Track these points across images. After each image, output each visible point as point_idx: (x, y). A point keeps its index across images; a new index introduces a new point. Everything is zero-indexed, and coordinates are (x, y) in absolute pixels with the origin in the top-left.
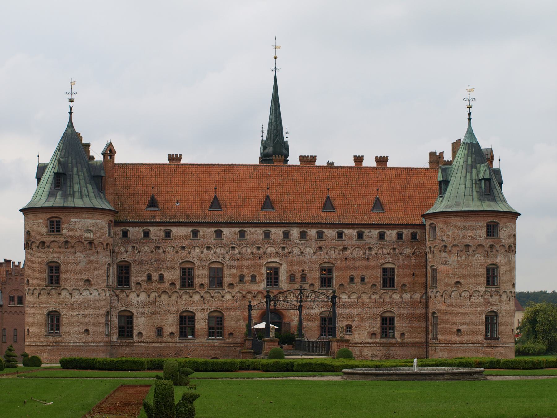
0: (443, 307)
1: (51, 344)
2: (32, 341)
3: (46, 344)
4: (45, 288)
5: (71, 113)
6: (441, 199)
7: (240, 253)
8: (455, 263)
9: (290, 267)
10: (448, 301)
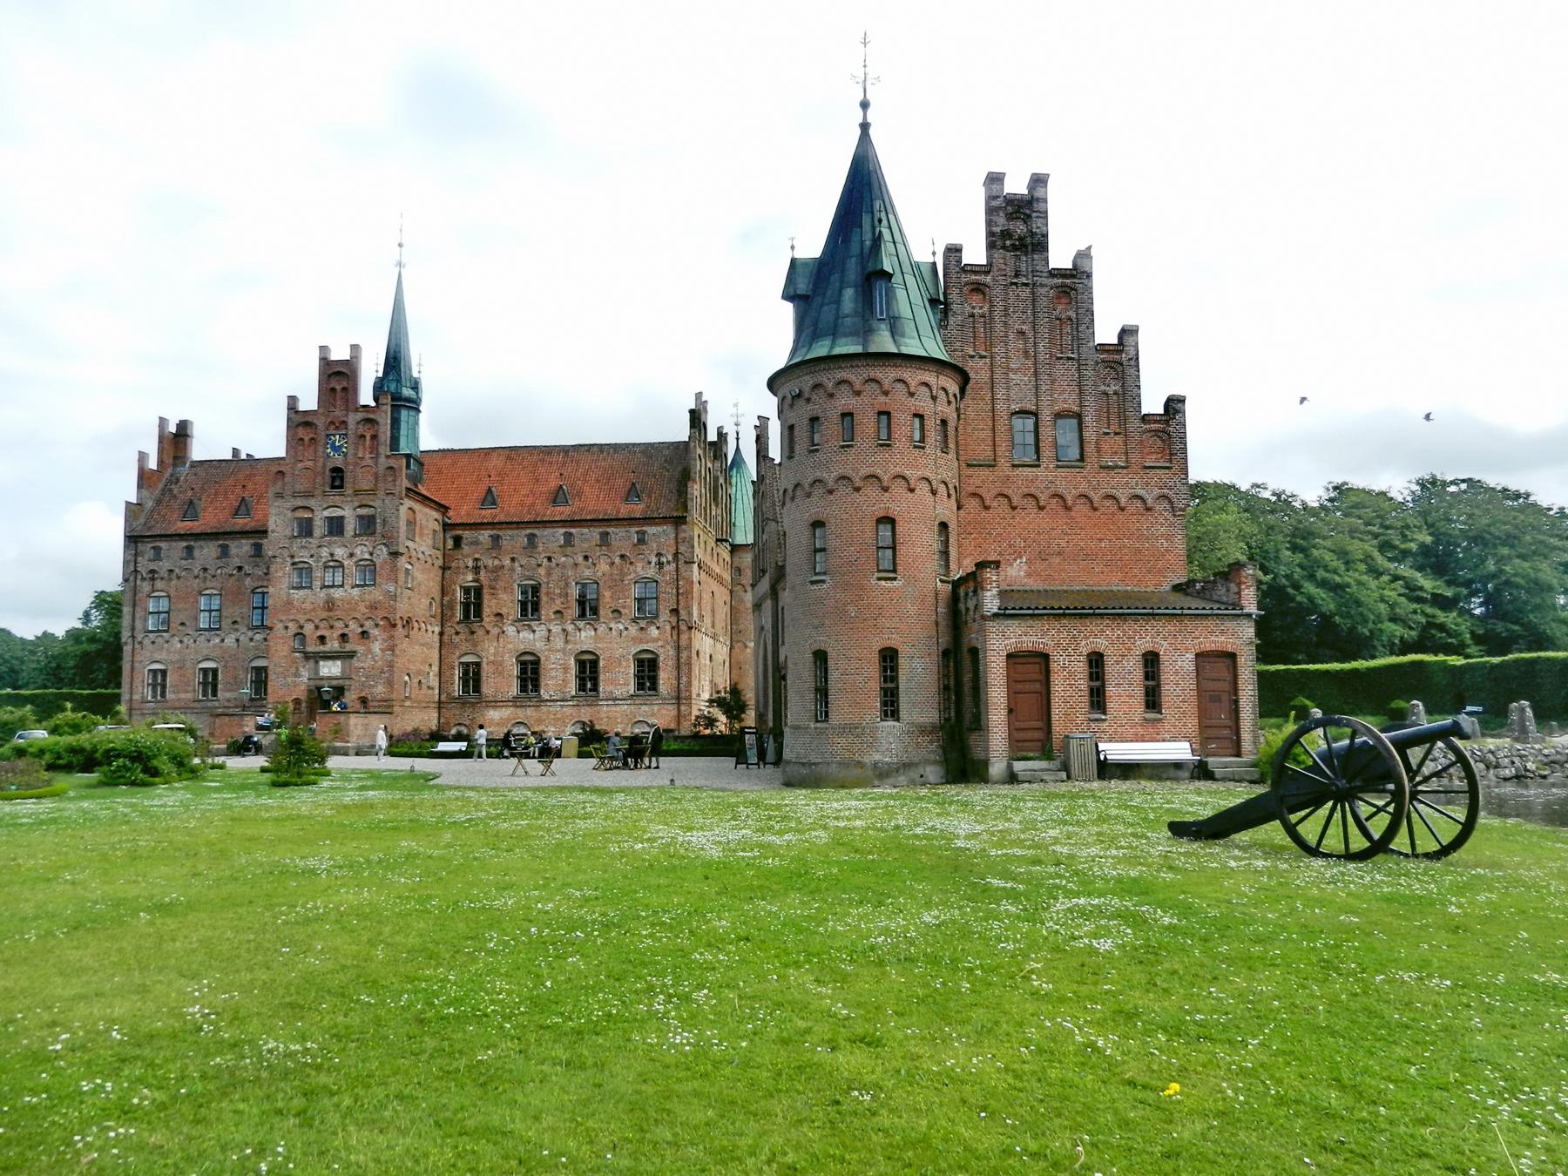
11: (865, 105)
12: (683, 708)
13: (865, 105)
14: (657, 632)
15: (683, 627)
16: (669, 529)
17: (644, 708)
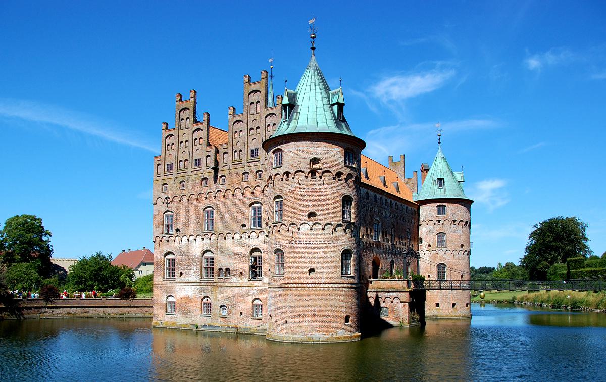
0: (453, 260)
1: (346, 286)
2: (323, 282)
3: (342, 285)
4: (342, 223)
6: (443, 190)
7: (366, 209)
8: (461, 232)
9: (382, 225)
10: (456, 257)
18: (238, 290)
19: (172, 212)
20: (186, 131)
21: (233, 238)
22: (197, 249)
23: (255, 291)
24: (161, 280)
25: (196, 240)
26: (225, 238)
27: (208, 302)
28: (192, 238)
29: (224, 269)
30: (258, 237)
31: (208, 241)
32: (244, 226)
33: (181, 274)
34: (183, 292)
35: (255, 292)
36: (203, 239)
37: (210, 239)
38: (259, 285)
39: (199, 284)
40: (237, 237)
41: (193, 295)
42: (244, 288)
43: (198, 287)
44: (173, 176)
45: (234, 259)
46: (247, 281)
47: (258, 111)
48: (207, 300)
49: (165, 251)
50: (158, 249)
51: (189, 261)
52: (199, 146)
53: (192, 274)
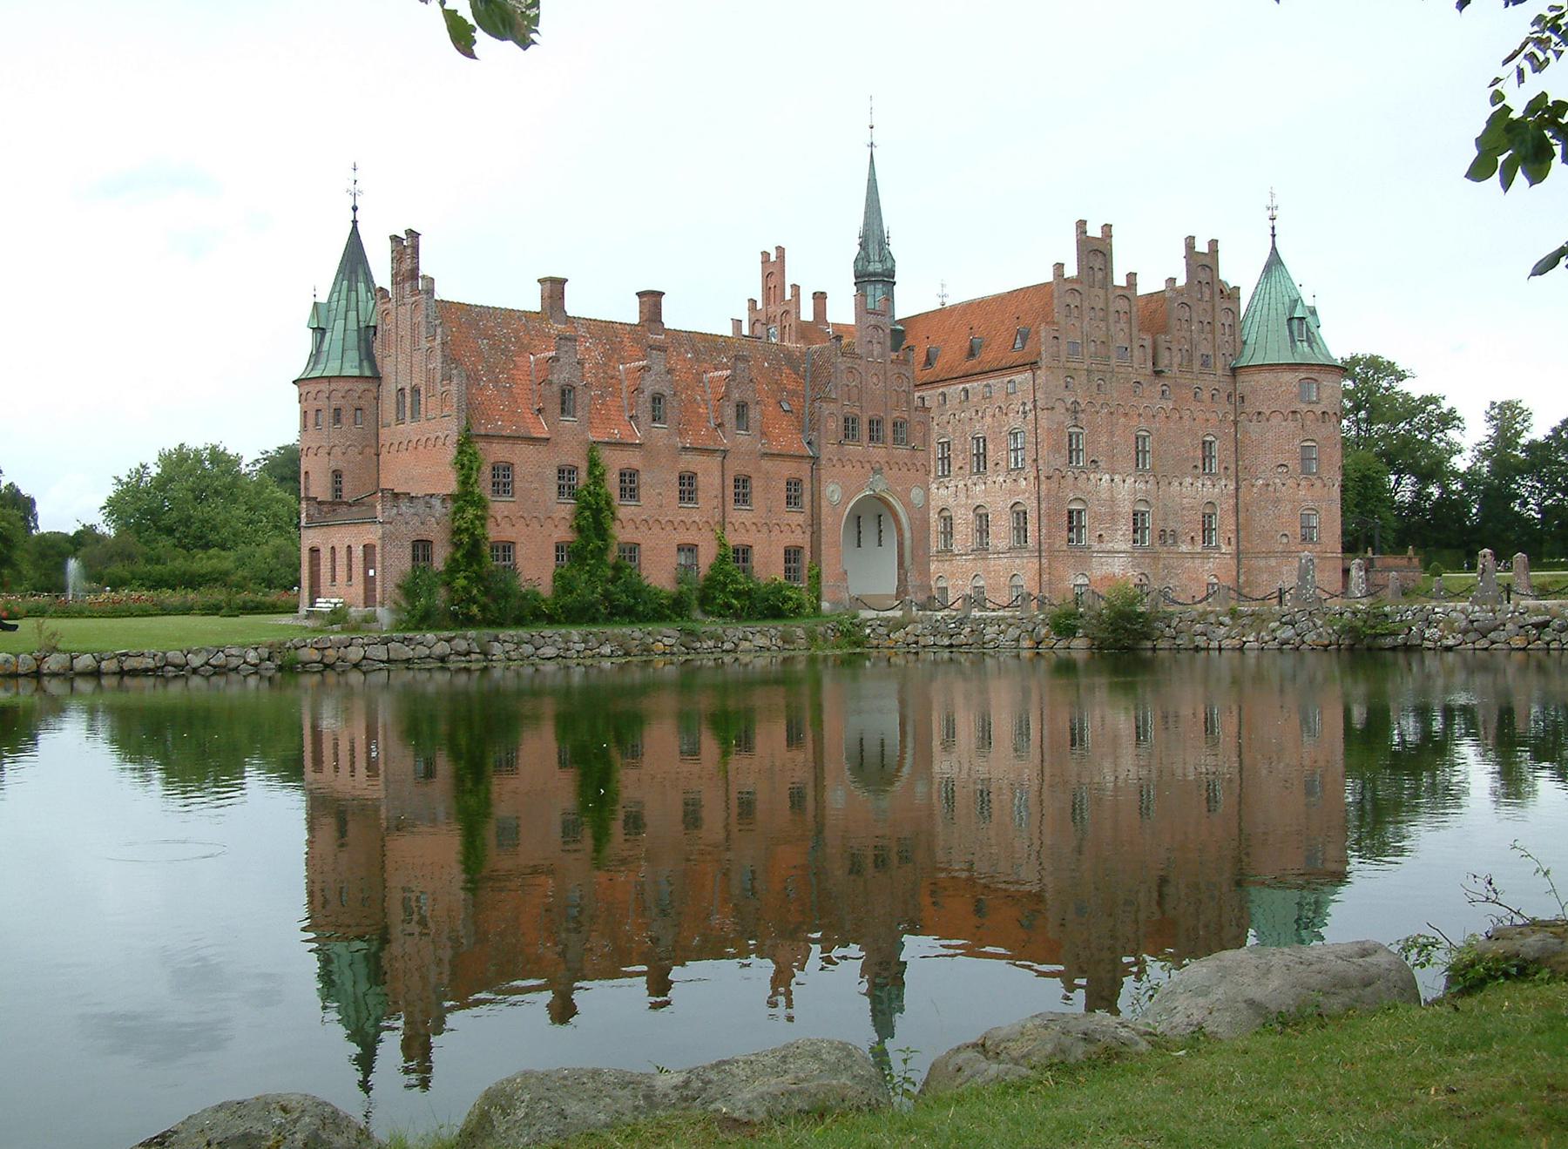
5: (1274, 236)
11: (355, 209)
12: (1044, 561)
13: (355, 209)
14: (1024, 483)
15: (1042, 478)
16: (1028, 375)
17: (1018, 561)
18: (1188, 564)
19: (1082, 428)
20: (1101, 293)
21: (1181, 484)
22: (1127, 497)
23: (1211, 565)
24: (1065, 548)
25: (1124, 481)
26: (1170, 483)
27: (1142, 583)
28: (1116, 477)
29: (1168, 531)
30: (1214, 485)
31: (1142, 486)
32: (1196, 467)
33: (1100, 535)
34: (1105, 567)
35: (1210, 565)
36: (1136, 482)
37: (1147, 482)
38: (1216, 555)
39: (1128, 555)
40: (1189, 480)
41: (1122, 572)
42: (1198, 562)
43: (1130, 559)
44: (1085, 367)
45: (1183, 516)
46: (1199, 551)
47: (1207, 299)
48: (1141, 580)
49: (1071, 497)
50: (1058, 492)
51: (1113, 517)
52: (1123, 325)
53: (1121, 540)
